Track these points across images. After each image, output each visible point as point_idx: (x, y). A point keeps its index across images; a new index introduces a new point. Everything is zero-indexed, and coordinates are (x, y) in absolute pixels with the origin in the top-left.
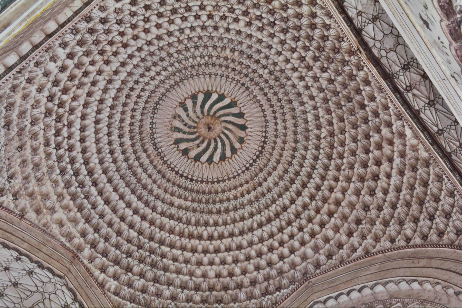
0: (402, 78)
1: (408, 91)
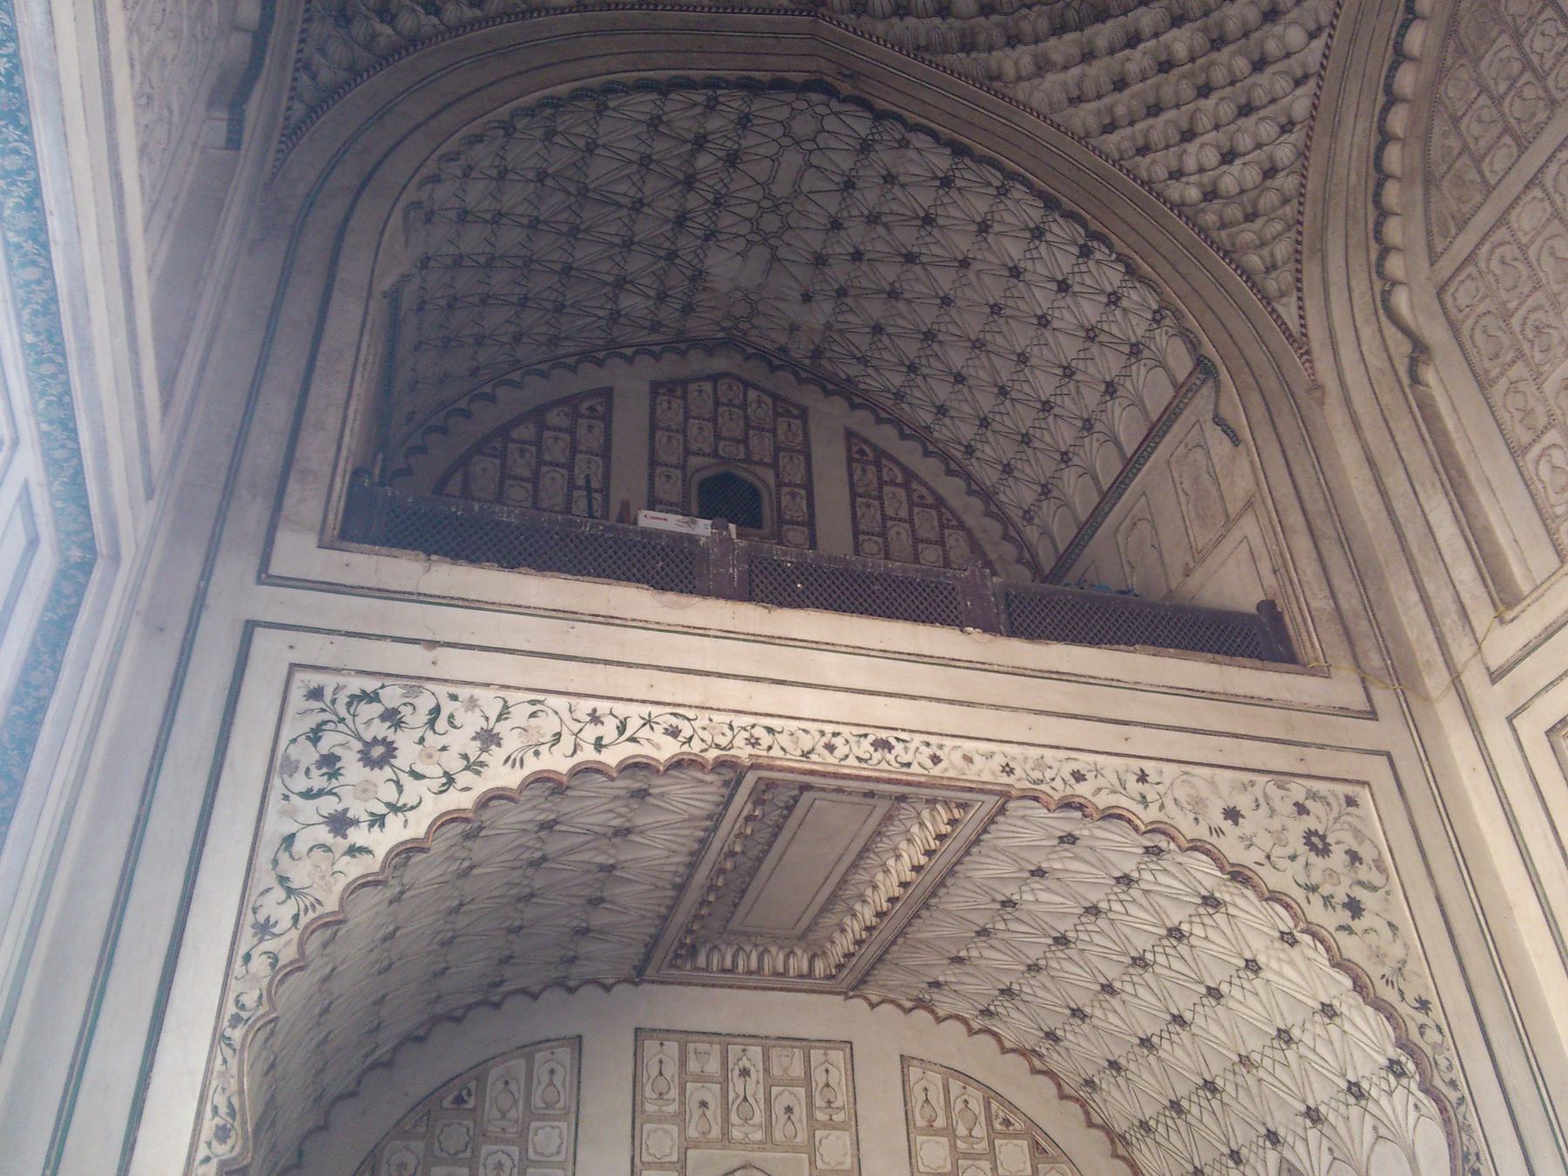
0: (734, 104)
1: (709, 100)
